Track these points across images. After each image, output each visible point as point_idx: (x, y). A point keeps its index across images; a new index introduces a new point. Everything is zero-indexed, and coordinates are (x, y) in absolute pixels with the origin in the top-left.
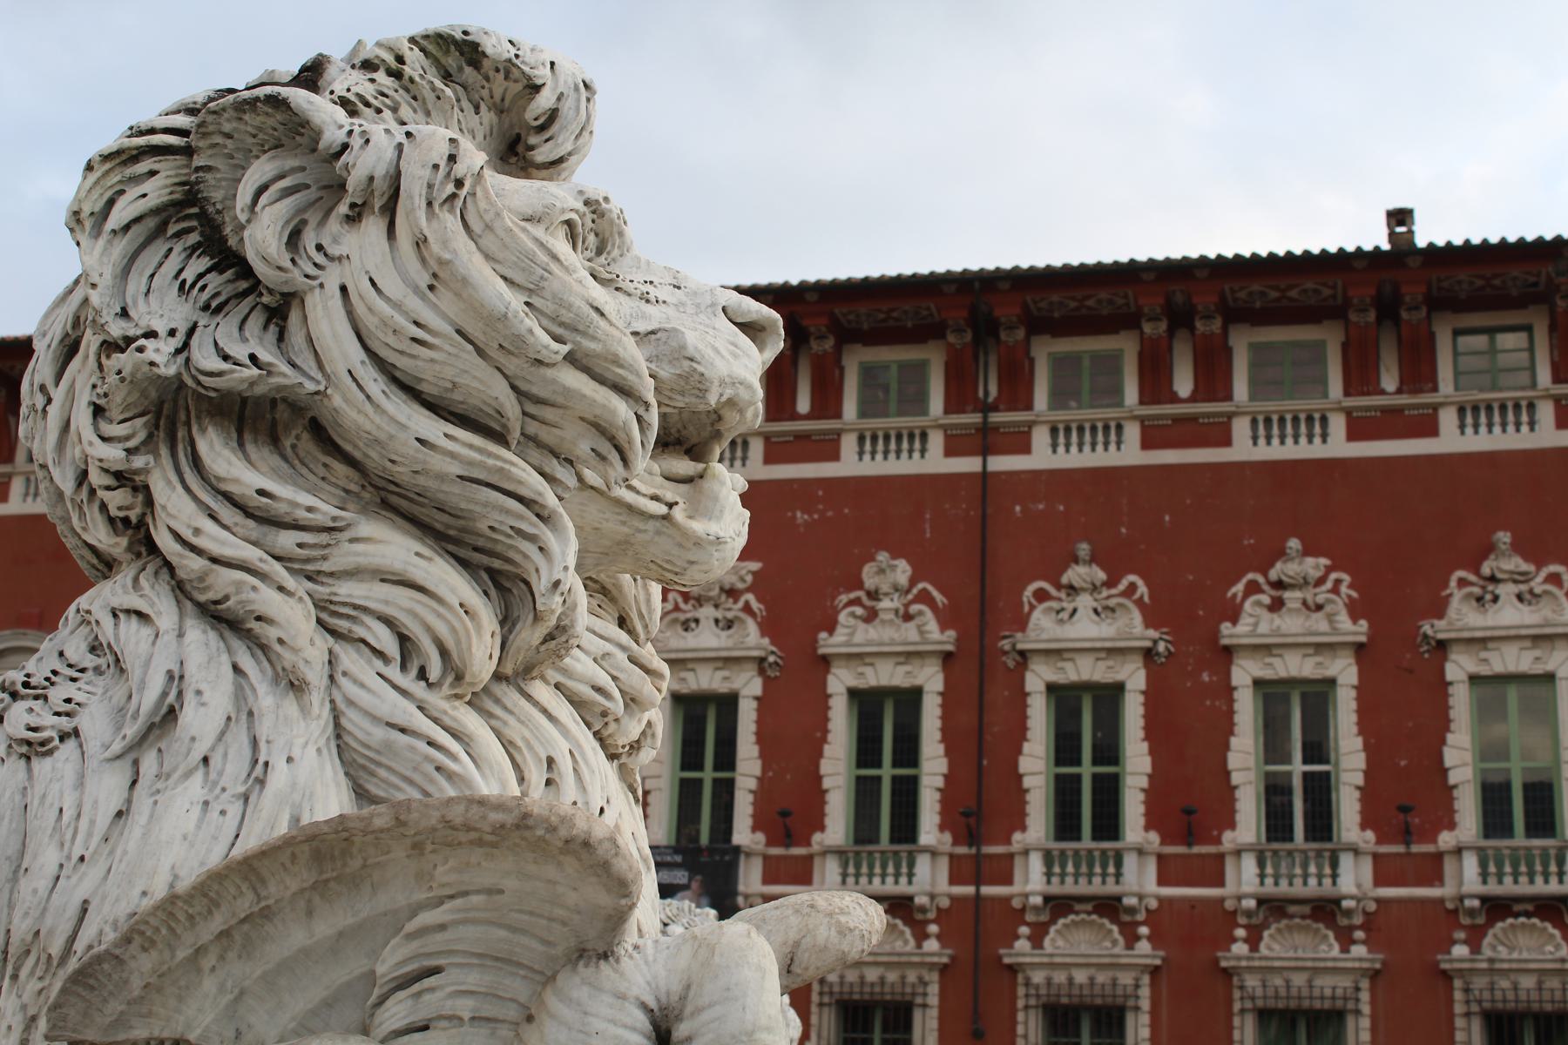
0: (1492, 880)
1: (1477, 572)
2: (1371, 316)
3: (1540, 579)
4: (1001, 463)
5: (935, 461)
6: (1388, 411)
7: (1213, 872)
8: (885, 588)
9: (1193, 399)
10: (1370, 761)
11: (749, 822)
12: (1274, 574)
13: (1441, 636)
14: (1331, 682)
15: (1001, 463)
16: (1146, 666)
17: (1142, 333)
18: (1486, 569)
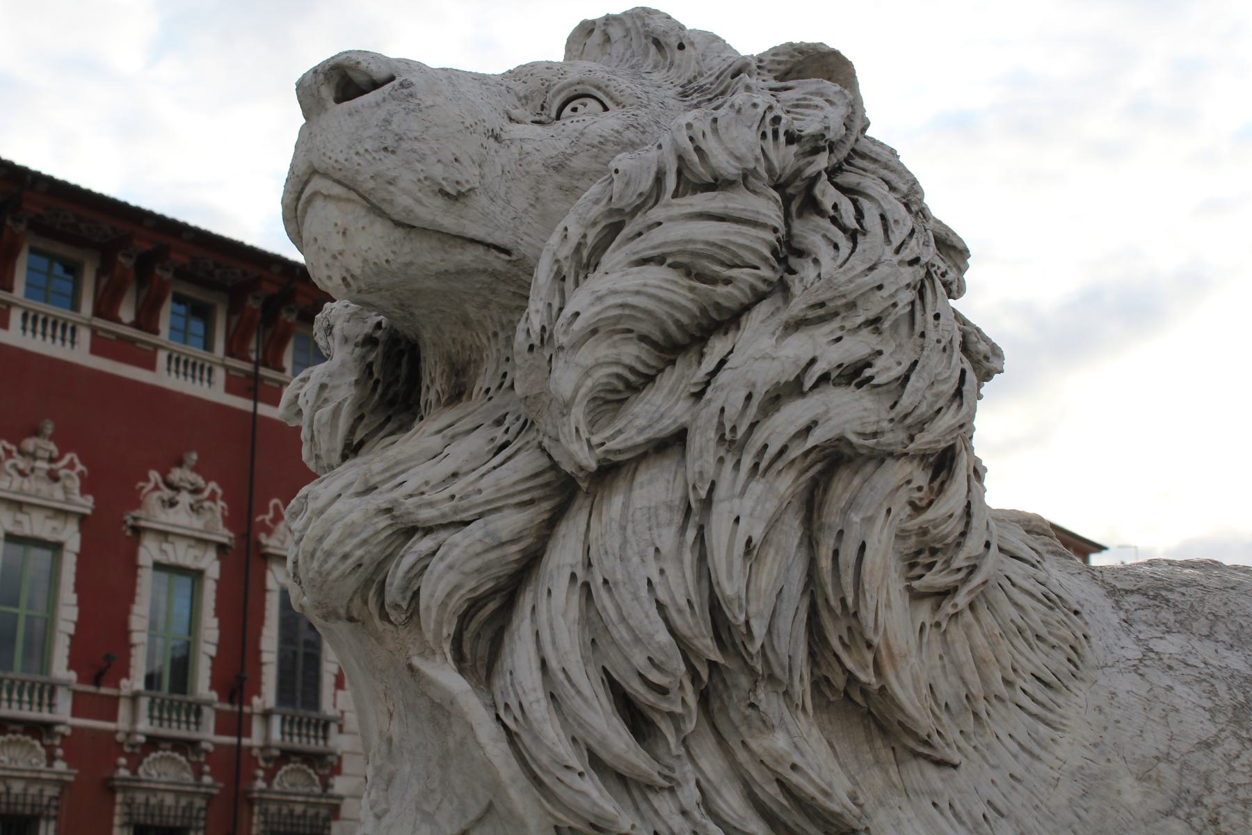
6: (121, 338)
10: (81, 614)
11: (65, 662)
16: (219, 558)
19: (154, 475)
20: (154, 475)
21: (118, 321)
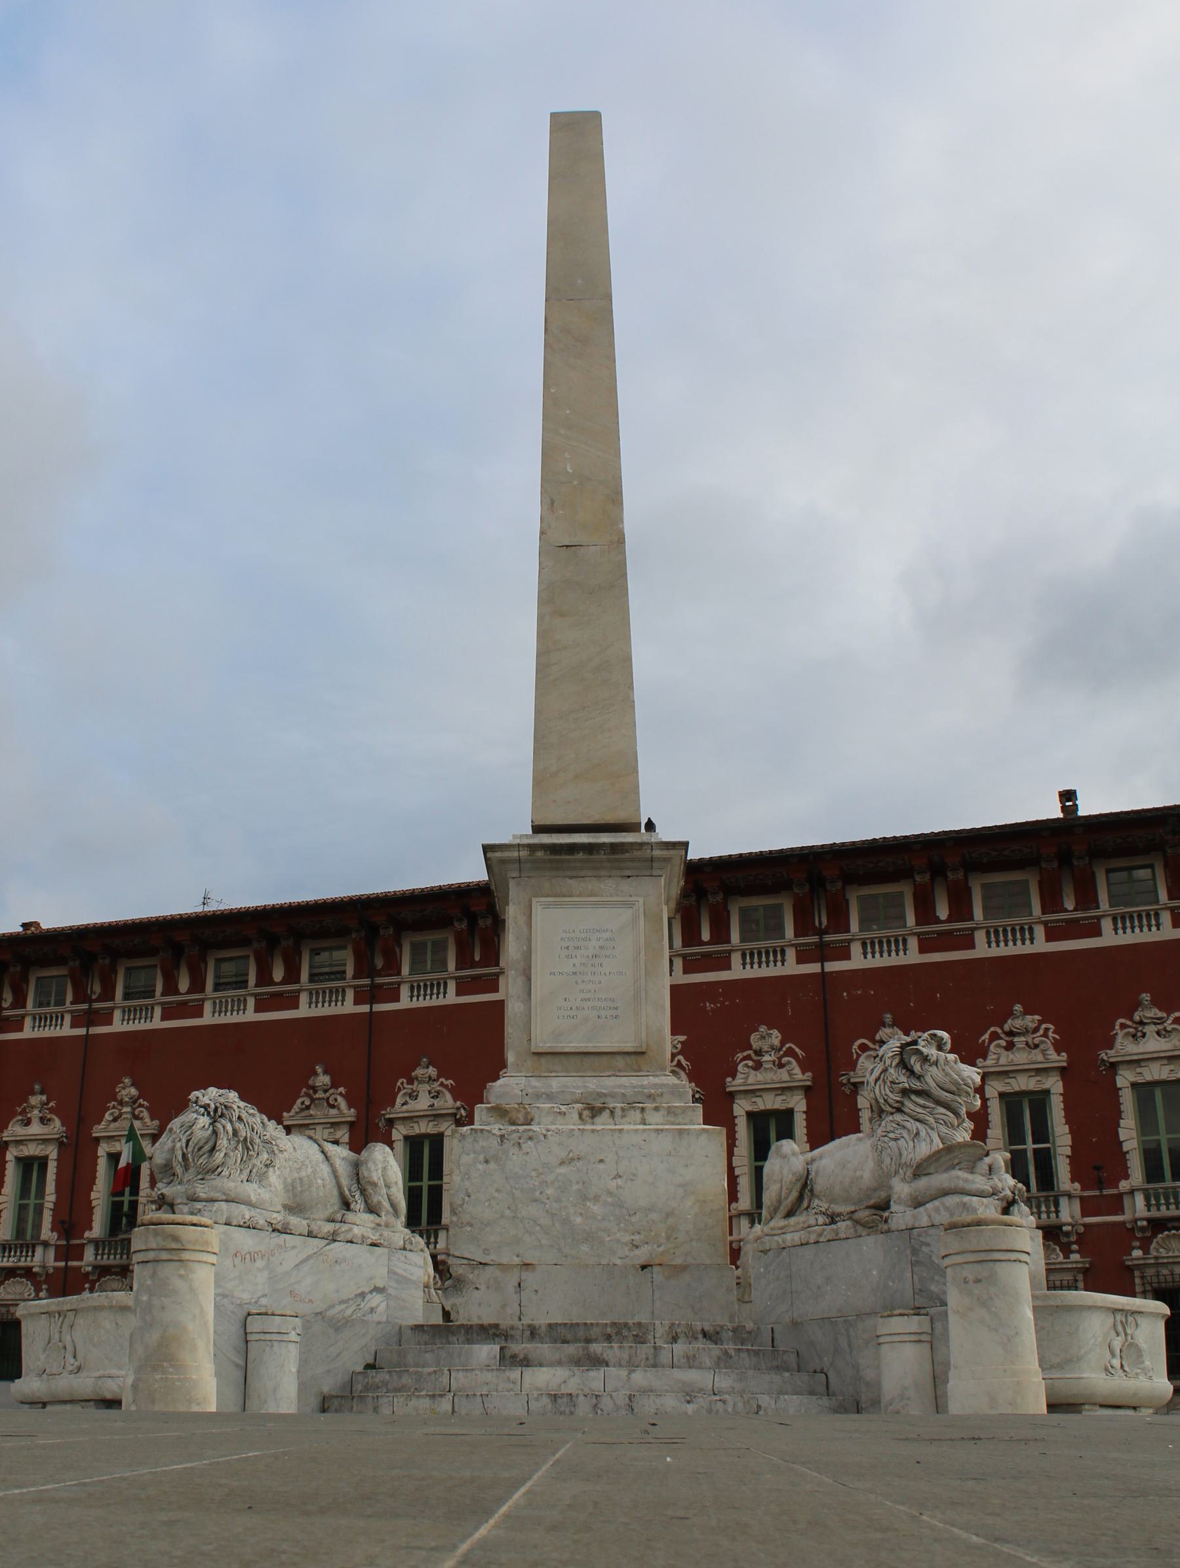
0: (1153, 1209)
1: (1131, 1019)
2: (1055, 864)
3: (1169, 1021)
4: (833, 966)
5: (791, 967)
7: (1116, 1204)
8: (765, 1048)
9: (948, 921)
12: (1007, 1027)
13: (1112, 1060)
14: (1047, 1092)
15: (833, 966)
17: (915, 881)
18: (1137, 1018)
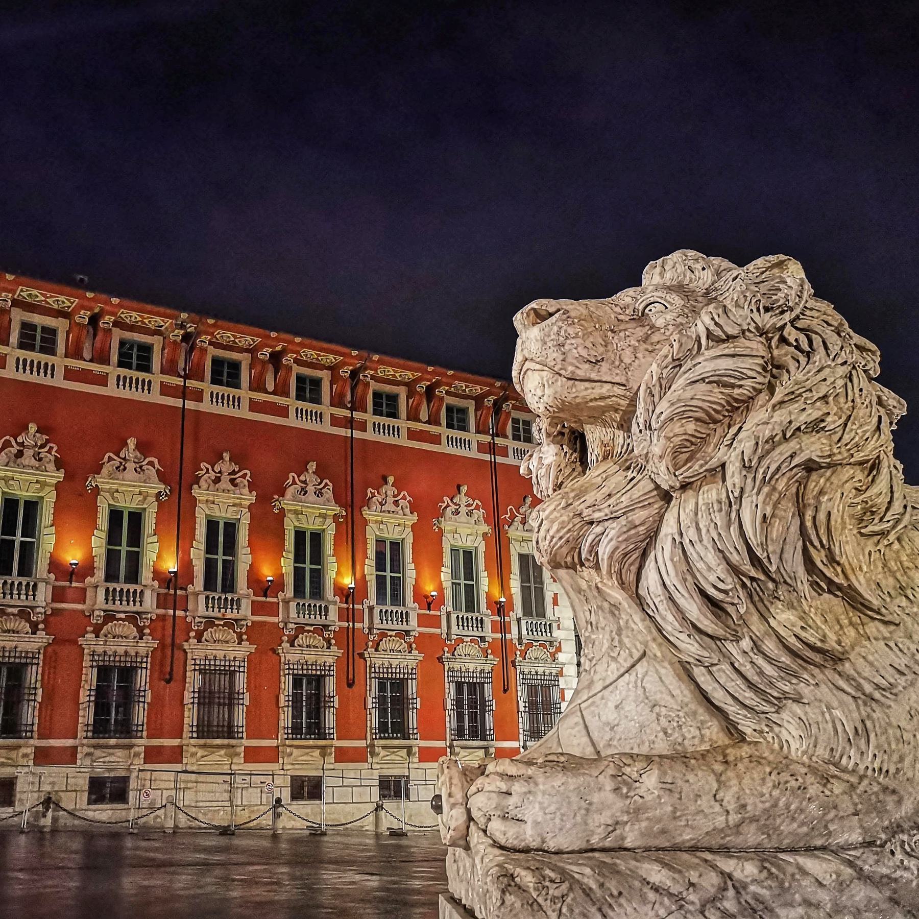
12: (20, 439)
19: (446, 499)
20: (446, 499)
21: (419, 421)
